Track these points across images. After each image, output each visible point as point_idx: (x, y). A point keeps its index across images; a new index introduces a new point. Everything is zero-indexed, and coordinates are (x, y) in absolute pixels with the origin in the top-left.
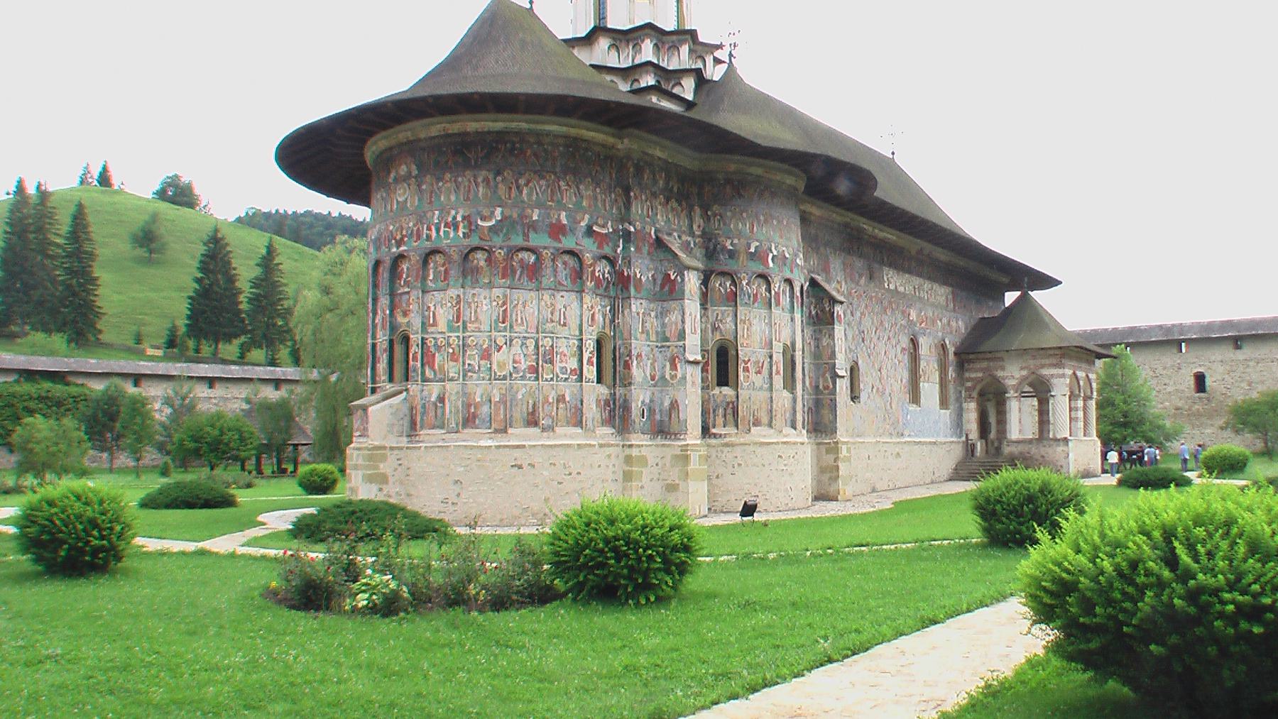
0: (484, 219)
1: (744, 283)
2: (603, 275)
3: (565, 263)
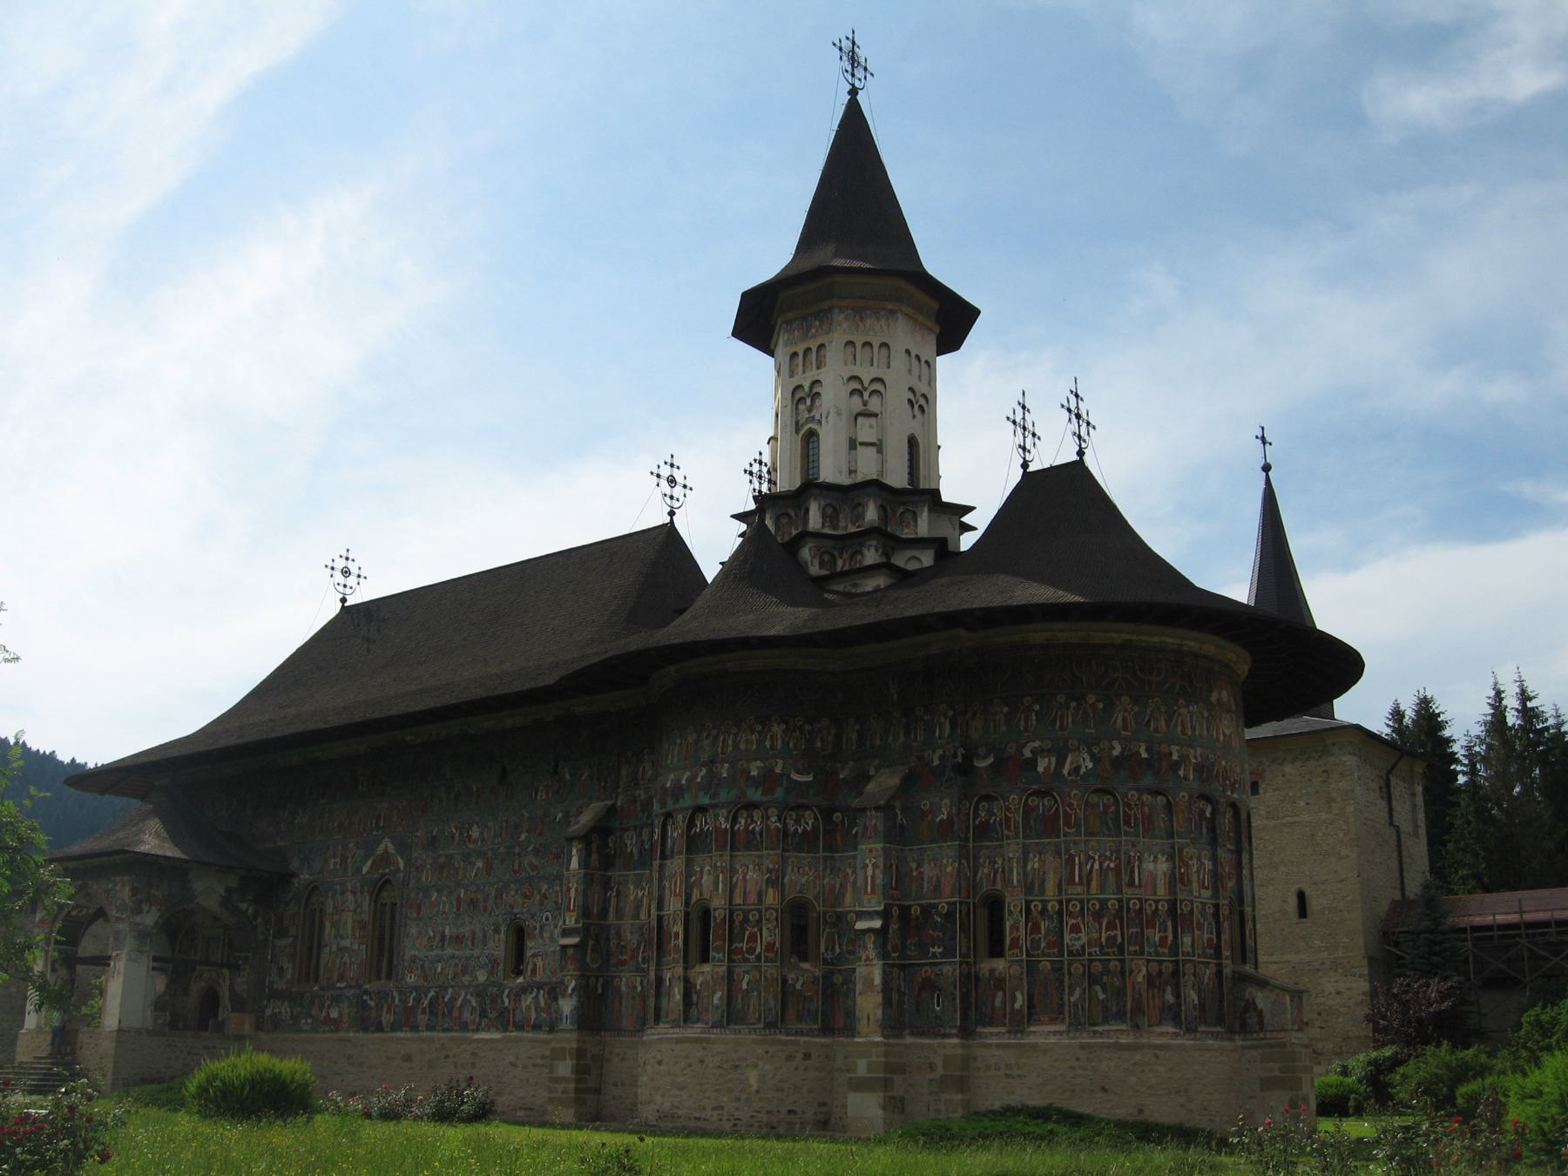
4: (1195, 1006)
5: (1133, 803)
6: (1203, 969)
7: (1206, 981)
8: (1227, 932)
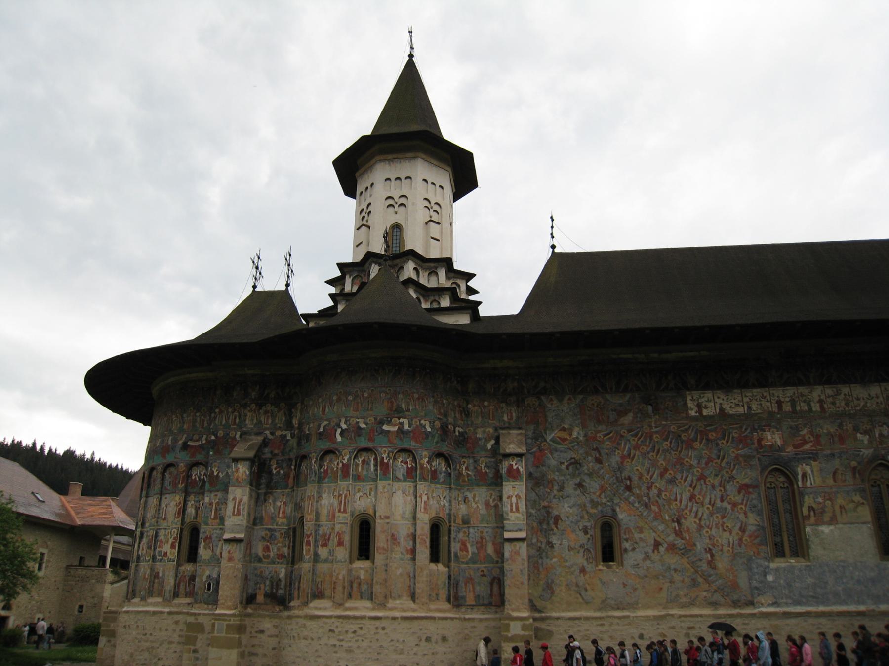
1: (313, 462)
2: (199, 477)
3: (170, 473)
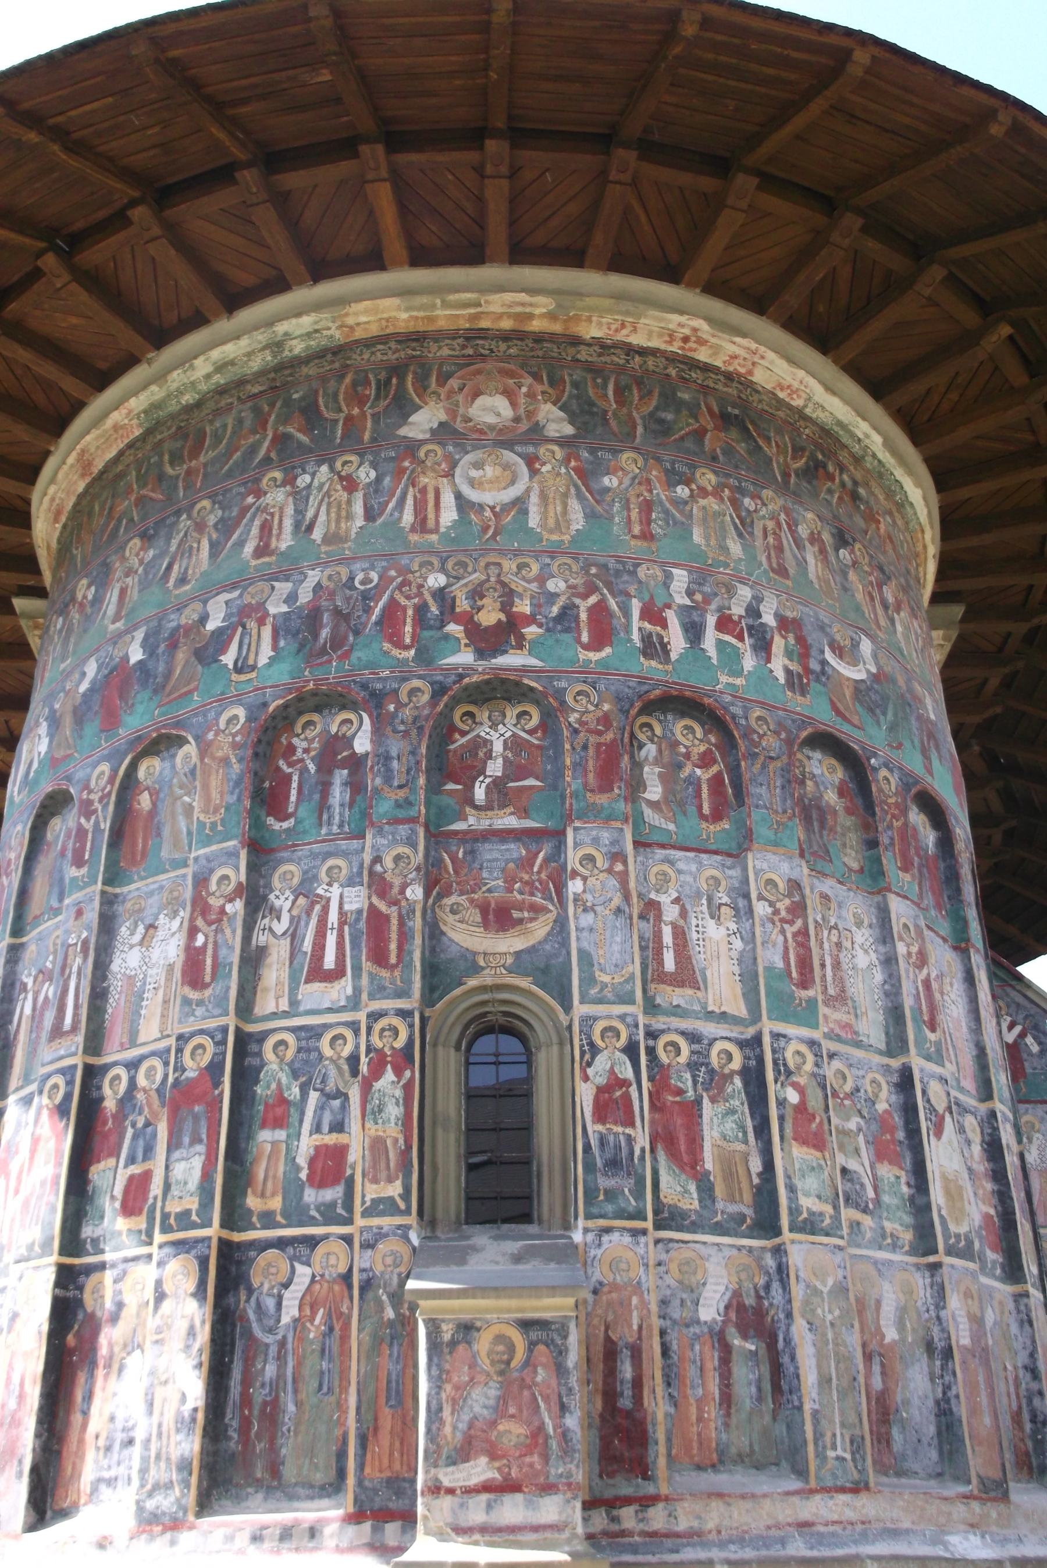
0: (839, 651)
4: (184, 1424)
5: (95, 797)
6: (285, 1266)
7: (290, 1311)
8: (394, 1111)
